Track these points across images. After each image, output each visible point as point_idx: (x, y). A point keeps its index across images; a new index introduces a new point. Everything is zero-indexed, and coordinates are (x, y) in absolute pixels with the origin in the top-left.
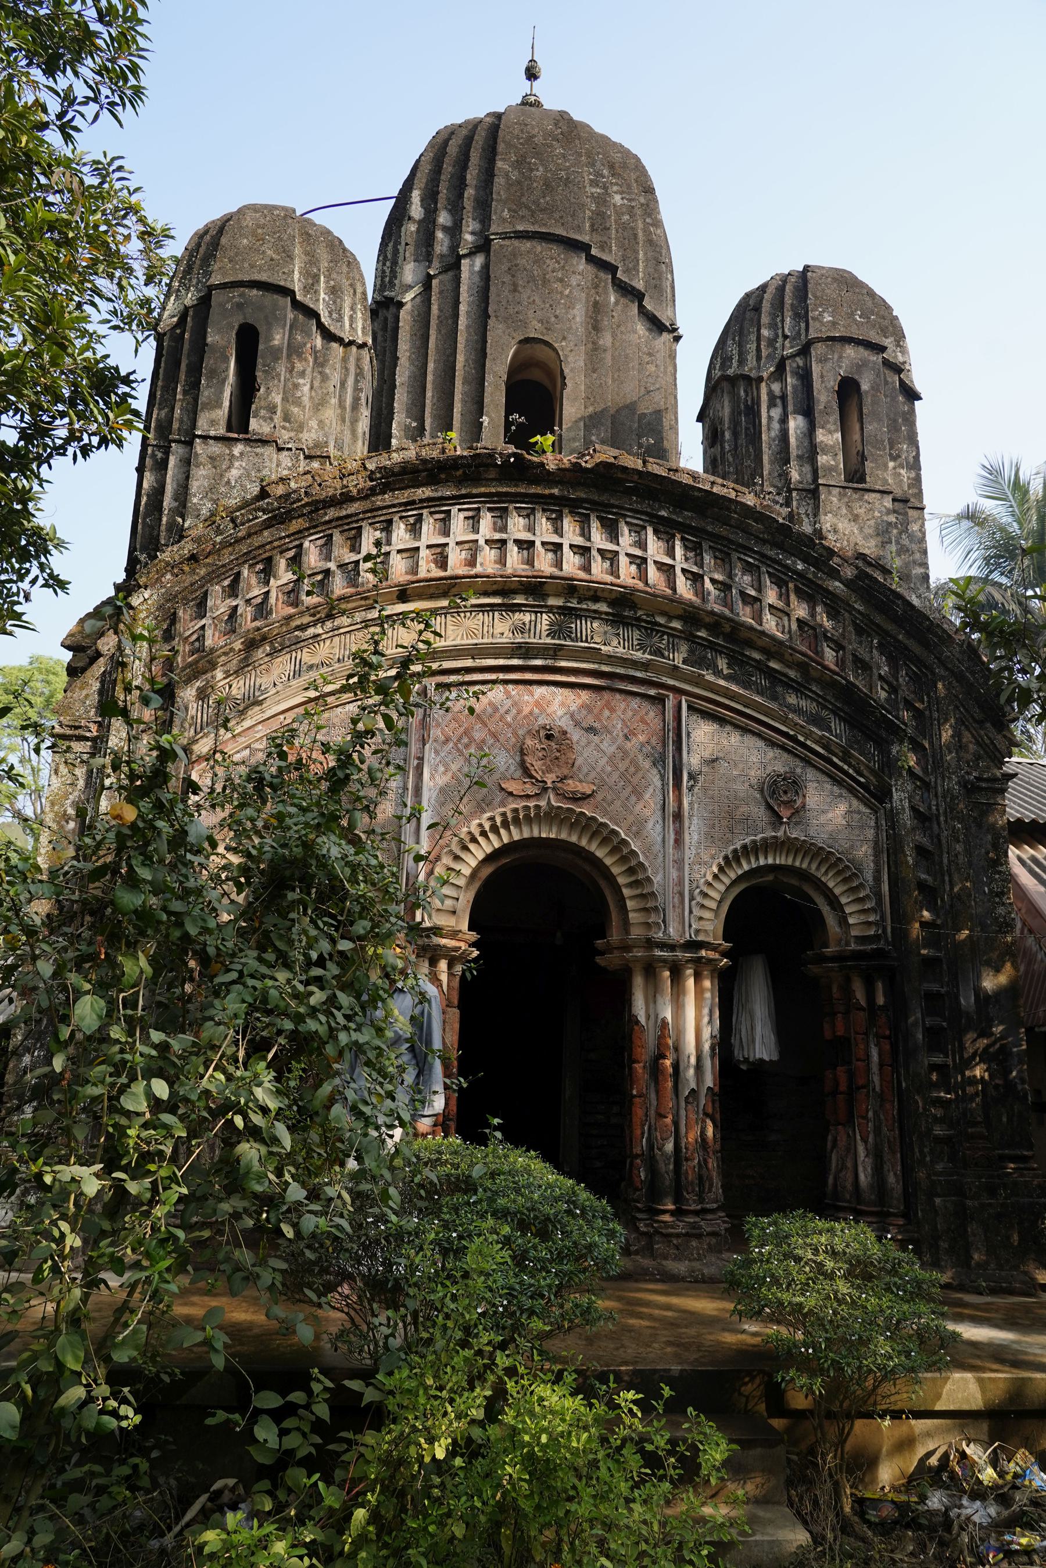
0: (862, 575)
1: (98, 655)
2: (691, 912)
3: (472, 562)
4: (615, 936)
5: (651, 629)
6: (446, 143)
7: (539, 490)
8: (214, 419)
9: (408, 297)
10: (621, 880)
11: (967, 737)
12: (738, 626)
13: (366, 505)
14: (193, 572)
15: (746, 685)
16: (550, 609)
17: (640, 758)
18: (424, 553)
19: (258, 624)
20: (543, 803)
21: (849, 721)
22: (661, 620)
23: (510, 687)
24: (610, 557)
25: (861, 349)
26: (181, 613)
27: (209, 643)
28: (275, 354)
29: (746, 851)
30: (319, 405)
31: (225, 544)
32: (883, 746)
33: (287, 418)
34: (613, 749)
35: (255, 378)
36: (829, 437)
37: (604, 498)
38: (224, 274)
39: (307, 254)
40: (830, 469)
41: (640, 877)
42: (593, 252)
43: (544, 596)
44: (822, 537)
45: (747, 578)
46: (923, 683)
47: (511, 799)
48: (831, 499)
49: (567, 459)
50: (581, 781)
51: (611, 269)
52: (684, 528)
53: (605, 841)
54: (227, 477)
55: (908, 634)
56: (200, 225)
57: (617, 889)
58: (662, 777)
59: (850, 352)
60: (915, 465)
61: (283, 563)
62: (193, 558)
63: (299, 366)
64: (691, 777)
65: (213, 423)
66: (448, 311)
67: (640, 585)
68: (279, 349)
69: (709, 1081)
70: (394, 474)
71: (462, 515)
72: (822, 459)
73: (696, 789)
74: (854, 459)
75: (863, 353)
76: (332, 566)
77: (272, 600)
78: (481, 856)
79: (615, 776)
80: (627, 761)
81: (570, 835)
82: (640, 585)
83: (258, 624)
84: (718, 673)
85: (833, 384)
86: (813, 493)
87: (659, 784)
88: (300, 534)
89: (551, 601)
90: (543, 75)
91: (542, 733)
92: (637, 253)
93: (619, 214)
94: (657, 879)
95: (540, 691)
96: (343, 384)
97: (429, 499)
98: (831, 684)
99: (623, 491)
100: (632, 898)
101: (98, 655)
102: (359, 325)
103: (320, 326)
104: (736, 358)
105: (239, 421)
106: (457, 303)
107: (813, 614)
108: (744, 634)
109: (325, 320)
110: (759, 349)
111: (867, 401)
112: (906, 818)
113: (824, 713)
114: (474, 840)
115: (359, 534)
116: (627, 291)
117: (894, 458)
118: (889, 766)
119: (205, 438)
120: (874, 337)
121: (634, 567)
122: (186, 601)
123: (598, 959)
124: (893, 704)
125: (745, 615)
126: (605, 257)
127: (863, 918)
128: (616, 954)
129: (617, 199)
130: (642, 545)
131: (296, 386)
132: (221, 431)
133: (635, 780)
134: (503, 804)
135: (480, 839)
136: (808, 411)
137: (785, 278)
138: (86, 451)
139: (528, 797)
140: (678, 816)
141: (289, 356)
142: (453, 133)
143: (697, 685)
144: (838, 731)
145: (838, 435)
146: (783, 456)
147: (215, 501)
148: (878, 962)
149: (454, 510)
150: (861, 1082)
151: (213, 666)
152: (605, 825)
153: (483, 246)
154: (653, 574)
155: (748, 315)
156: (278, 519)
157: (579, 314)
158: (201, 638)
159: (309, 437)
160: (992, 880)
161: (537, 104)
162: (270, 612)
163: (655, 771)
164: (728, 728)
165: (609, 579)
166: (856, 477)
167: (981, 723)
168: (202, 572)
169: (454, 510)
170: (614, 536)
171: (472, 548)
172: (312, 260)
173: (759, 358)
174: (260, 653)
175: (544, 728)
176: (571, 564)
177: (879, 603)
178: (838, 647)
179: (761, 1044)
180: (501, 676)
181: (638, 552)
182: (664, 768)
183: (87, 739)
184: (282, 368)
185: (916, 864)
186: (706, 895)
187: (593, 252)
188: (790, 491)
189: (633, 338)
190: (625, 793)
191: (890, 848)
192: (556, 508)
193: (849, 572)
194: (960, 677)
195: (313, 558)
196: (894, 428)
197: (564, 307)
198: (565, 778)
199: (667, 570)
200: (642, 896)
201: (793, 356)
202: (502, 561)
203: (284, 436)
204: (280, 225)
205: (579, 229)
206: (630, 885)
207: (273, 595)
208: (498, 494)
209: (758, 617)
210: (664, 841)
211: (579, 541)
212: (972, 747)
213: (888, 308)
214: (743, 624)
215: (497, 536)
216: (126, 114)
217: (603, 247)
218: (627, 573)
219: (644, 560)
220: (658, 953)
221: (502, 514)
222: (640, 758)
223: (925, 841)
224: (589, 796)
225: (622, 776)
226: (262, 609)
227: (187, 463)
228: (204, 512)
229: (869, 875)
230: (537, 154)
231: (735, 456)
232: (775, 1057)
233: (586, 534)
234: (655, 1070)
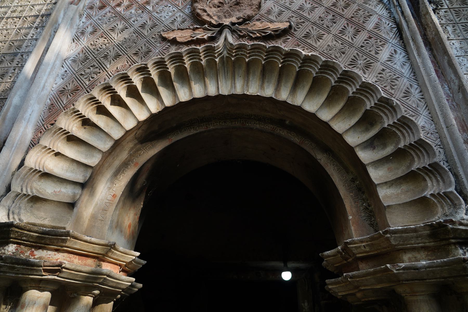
4: (356, 233)
123: (332, 285)
128: (364, 268)
135: (128, 101)
200: (400, 155)
206: (369, 144)
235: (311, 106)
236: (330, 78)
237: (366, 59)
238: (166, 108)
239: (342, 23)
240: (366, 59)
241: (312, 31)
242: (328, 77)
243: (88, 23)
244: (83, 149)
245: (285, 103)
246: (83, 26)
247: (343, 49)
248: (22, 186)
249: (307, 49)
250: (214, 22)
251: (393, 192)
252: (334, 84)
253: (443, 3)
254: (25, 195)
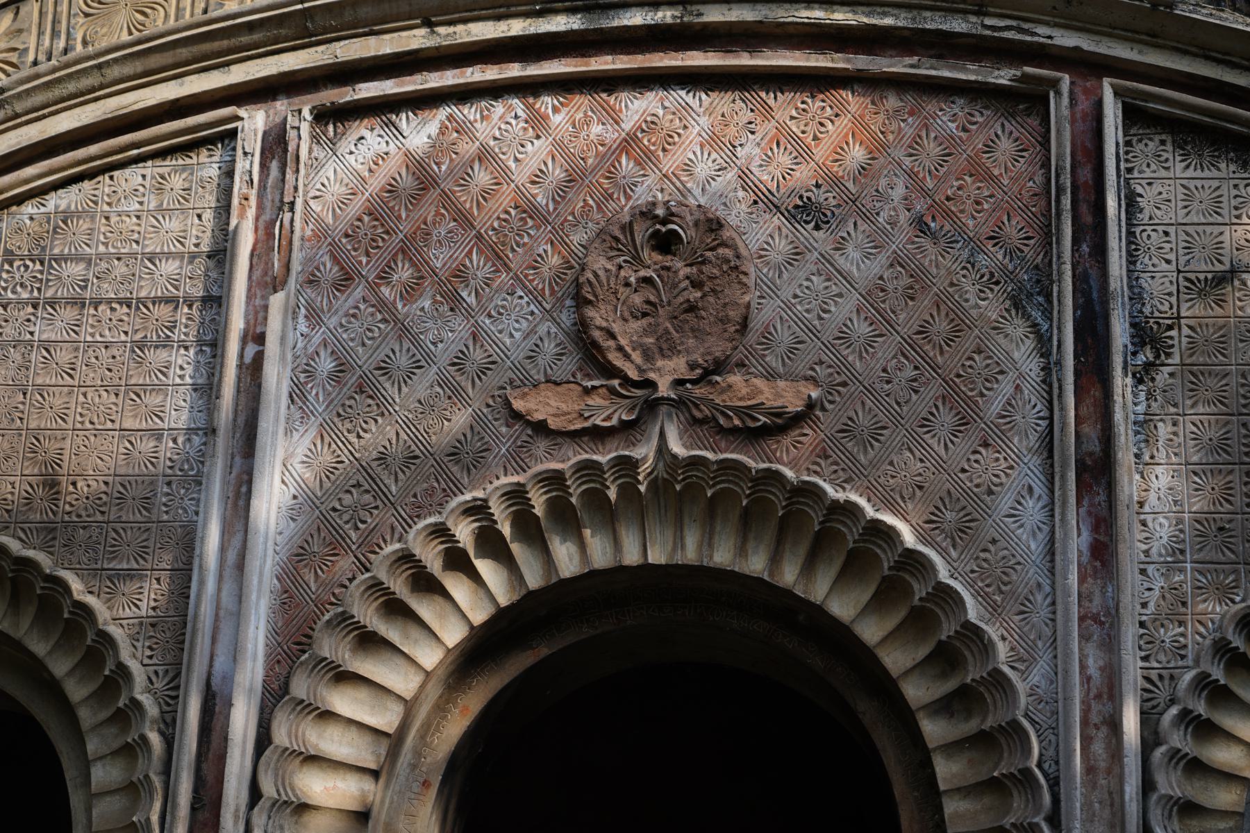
2: (1148, 786)
10: (916, 692)
17: (971, 290)
20: (644, 451)
23: (546, 102)
34: (877, 266)
41: (973, 674)
47: (541, 445)
50: (771, 376)
58: (1044, 345)
64: (1143, 335)
73: (1162, 376)
78: (453, 635)
79: (885, 351)
80: (927, 302)
81: (742, 551)
87: (1032, 367)
91: (641, 232)
95: (636, 107)
100: (953, 748)
114: (427, 584)
134: (517, 461)
139: (598, 435)
140: (1098, 471)
143: (1154, 39)
163: (1018, 328)
175: (647, 213)
180: (514, 70)
182: (1048, 314)
190: (920, 404)
198: (719, 366)
200: (984, 741)
210: (1051, 553)
222: (971, 290)
224: (797, 420)
225: (909, 348)
235: (842, 608)
236: (883, 556)
237: (964, 508)
238: (531, 594)
239: (931, 394)
240: (964, 508)
241: (860, 414)
242: (878, 551)
243: (317, 339)
244: (363, 693)
245: (788, 593)
246: (305, 348)
247: (920, 475)
248: (276, 785)
249: (843, 469)
250: (633, 374)
251: (968, 806)
252: (887, 572)
253: (1173, 346)
254: (285, 802)
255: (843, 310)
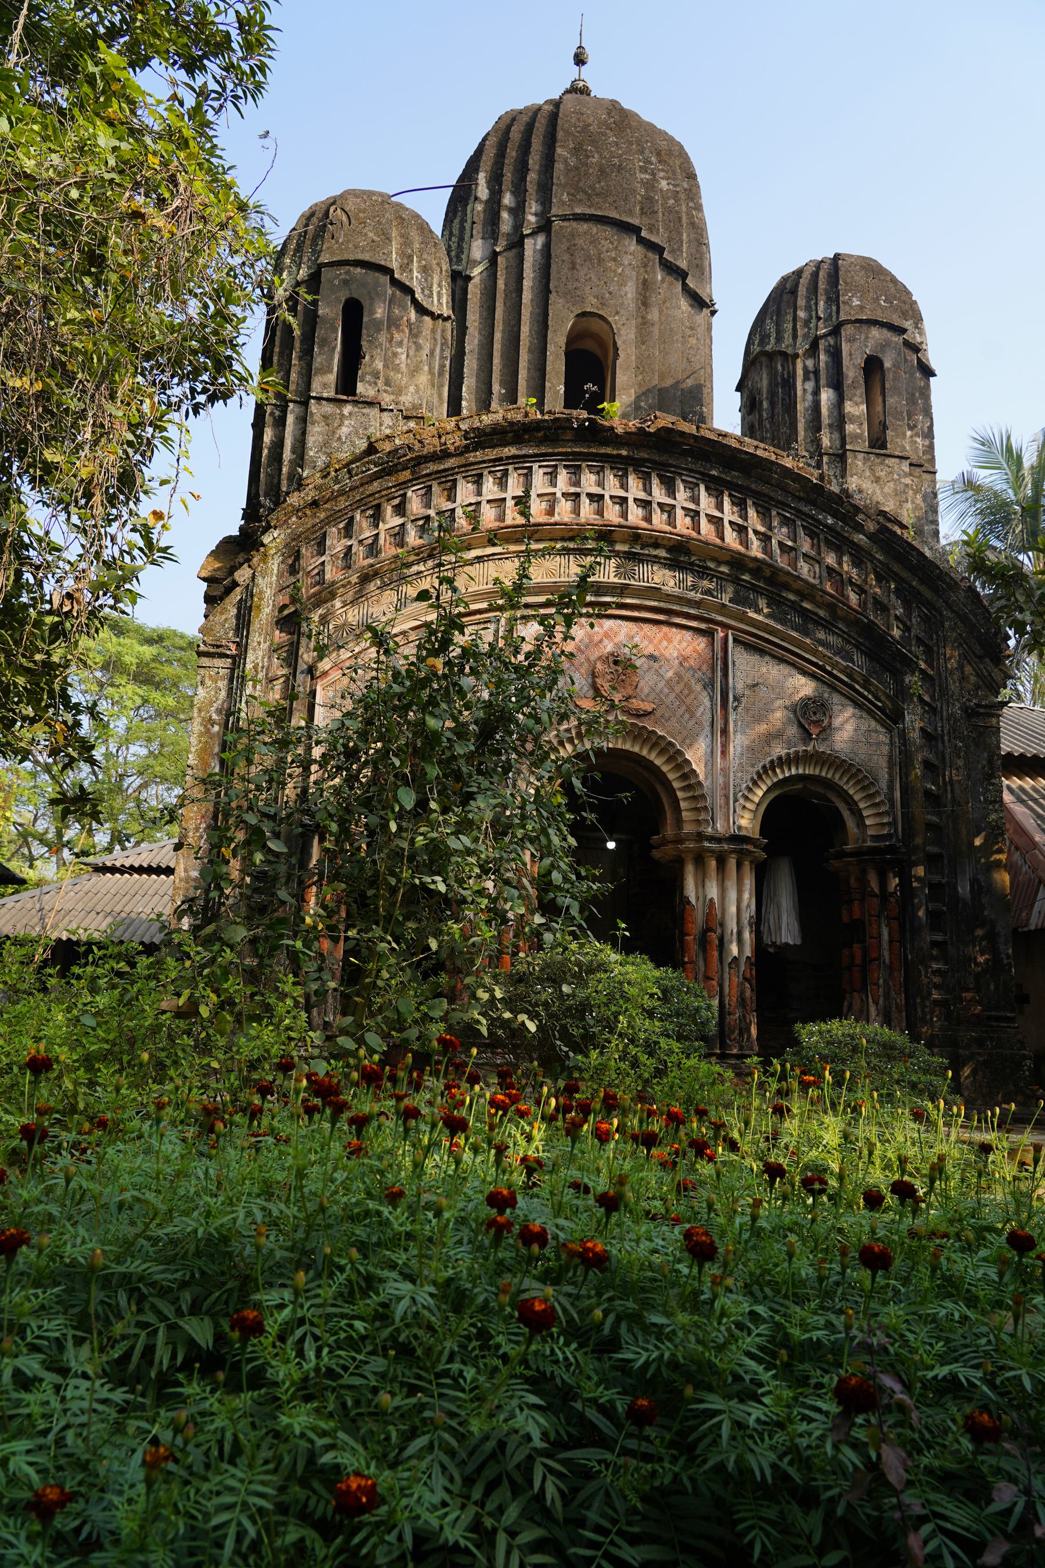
0: (883, 529)
1: (235, 584)
3: (551, 512)
4: (669, 831)
5: (702, 572)
6: (509, 127)
7: (609, 450)
8: (325, 383)
9: (476, 272)
10: (676, 785)
11: (968, 669)
12: (776, 570)
13: (460, 460)
14: (314, 515)
15: (783, 622)
16: (617, 554)
18: (510, 503)
19: (371, 561)
21: (869, 654)
22: (712, 565)
24: (669, 510)
25: (885, 331)
26: (303, 551)
27: (328, 576)
28: (377, 326)
29: (782, 762)
30: (414, 371)
31: (342, 493)
32: (897, 676)
33: (387, 383)
35: (360, 347)
36: (856, 408)
37: (664, 458)
38: (332, 254)
39: (402, 236)
40: (856, 437)
42: (643, 234)
43: (612, 543)
44: (849, 496)
45: (784, 530)
46: (932, 623)
48: (857, 463)
49: (633, 424)
51: (658, 249)
52: (731, 486)
53: (662, 752)
54: (339, 433)
55: (922, 581)
56: (305, 207)
57: (672, 792)
58: (711, 699)
59: (875, 333)
60: (929, 434)
61: (389, 510)
62: (315, 504)
63: (397, 337)
64: (736, 699)
65: (325, 386)
66: (513, 286)
67: (694, 534)
68: (381, 322)
69: (748, 952)
70: (486, 434)
71: (542, 471)
72: (850, 428)
74: (877, 428)
75: (886, 334)
76: (432, 513)
77: (381, 541)
79: (672, 696)
82: (694, 534)
83: (371, 561)
84: (758, 611)
85: (860, 361)
86: (840, 457)
87: (708, 704)
88: (404, 485)
89: (619, 547)
90: (590, 61)
92: (681, 234)
93: (665, 199)
94: (706, 784)
96: (432, 352)
97: (514, 457)
98: (857, 622)
99: (672, 451)
101: (235, 584)
102: (444, 300)
103: (415, 302)
104: (773, 335)
105: (347, 384)
106: (520, 278)
107: (840, 563)
108: (783, 578)
109: (418, 296)
110: (795, 329)
111: (889, 376)
112: (915, 736)
113: (848, 647)
115: (454, 486)
116: (672, 270)
117: (911, 428)
118: (902, 693)
119: (319, 399)
120: (896, 320)
121: (688, 520)
122: (308, 541)
124: (905, 640)
125: (781, 561)
126: (653, 239)
127: (877, 820)
129: (664, 184)
130: (695, 500)
131: (395, 354)
132: (331, 394)
133: (688, 701)
136: (837, 384)
137: (819, 264)
138: (196, 409)
140: (725, 732)
141: (389, 328)
142: (514, 119)
143: (741, 621)
144: (859, 663)
145: (864, 407)
146: (815, 424)
147: (329, 455)
148: (888, 857)
149: (535, 466)
150: (874, 955)
151: (333, 596)
152: (663, 737)
153: (545, 227)
154: (705, 526)
155: (786, 297)
156: (386, 472)
157: (630, 291)
158: (322, 573)
159: (407, 399)
160: (987, 790)
161: (585, 91)
162: (379, 552)
164: (767, 658)
165: (668, 528)
166: (878, 443)
167: (980, 658)
168: (322, 515)
169: (535, 466)
170: (671, 492)
171: (551, 500)
172: (407, 242)
173: (795, 336)
174: (372, 586)
176: (635, 515)
177: (897, 554)
178: (861, 590)
179: (787, 931)
181: (692, 506)
183: (227, 656)
184: (383, 337)
185: (924, 776)
186: (746, 798)
187: (643, 234)
188: (821, 455)
189: (677, 313)
191: (902, 759)
192: (622, 466)
193: (871, 527)
194: (964, 619)
195: (415, 506)
196: (912, 401)
197: (615, 283)
199: (717, 522)
200: (694, 798)
201: (825, 336)
202: (576, 511)
203: (386, 399)
204: (381, 210)
205: (630, 212)
207: (382, 536)
208: (573, 453)
209: (794, 564)
211: (642, 495)
212: (973, 679)
213: (909, 293)
214: (781, 570)
215: (572, 490)
216: (247, 106)
217: (650, 230)
218: (683, 523)
219: (697, 513)
220: (707, 844)
221: (576, 472)
223: (931, 757)
225: (678, 697)
226: (373, 549)
227: (303, 421)
228: (320, 464)
229: (883, 784)
230: (593, 143)
231: (772, 423)
232: (798, 942)
233: (648, 490)
234: (703, 942)
235: (658, 762)
255: (661, 684)
